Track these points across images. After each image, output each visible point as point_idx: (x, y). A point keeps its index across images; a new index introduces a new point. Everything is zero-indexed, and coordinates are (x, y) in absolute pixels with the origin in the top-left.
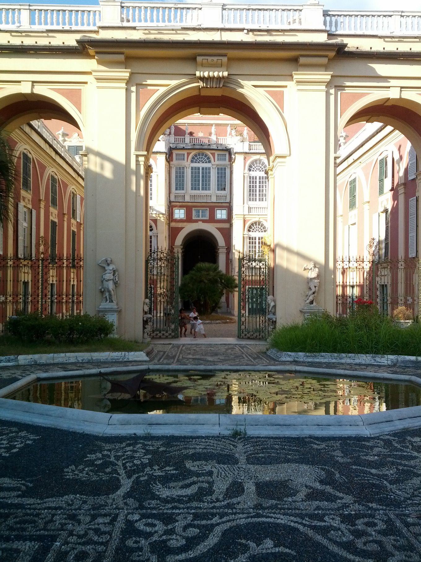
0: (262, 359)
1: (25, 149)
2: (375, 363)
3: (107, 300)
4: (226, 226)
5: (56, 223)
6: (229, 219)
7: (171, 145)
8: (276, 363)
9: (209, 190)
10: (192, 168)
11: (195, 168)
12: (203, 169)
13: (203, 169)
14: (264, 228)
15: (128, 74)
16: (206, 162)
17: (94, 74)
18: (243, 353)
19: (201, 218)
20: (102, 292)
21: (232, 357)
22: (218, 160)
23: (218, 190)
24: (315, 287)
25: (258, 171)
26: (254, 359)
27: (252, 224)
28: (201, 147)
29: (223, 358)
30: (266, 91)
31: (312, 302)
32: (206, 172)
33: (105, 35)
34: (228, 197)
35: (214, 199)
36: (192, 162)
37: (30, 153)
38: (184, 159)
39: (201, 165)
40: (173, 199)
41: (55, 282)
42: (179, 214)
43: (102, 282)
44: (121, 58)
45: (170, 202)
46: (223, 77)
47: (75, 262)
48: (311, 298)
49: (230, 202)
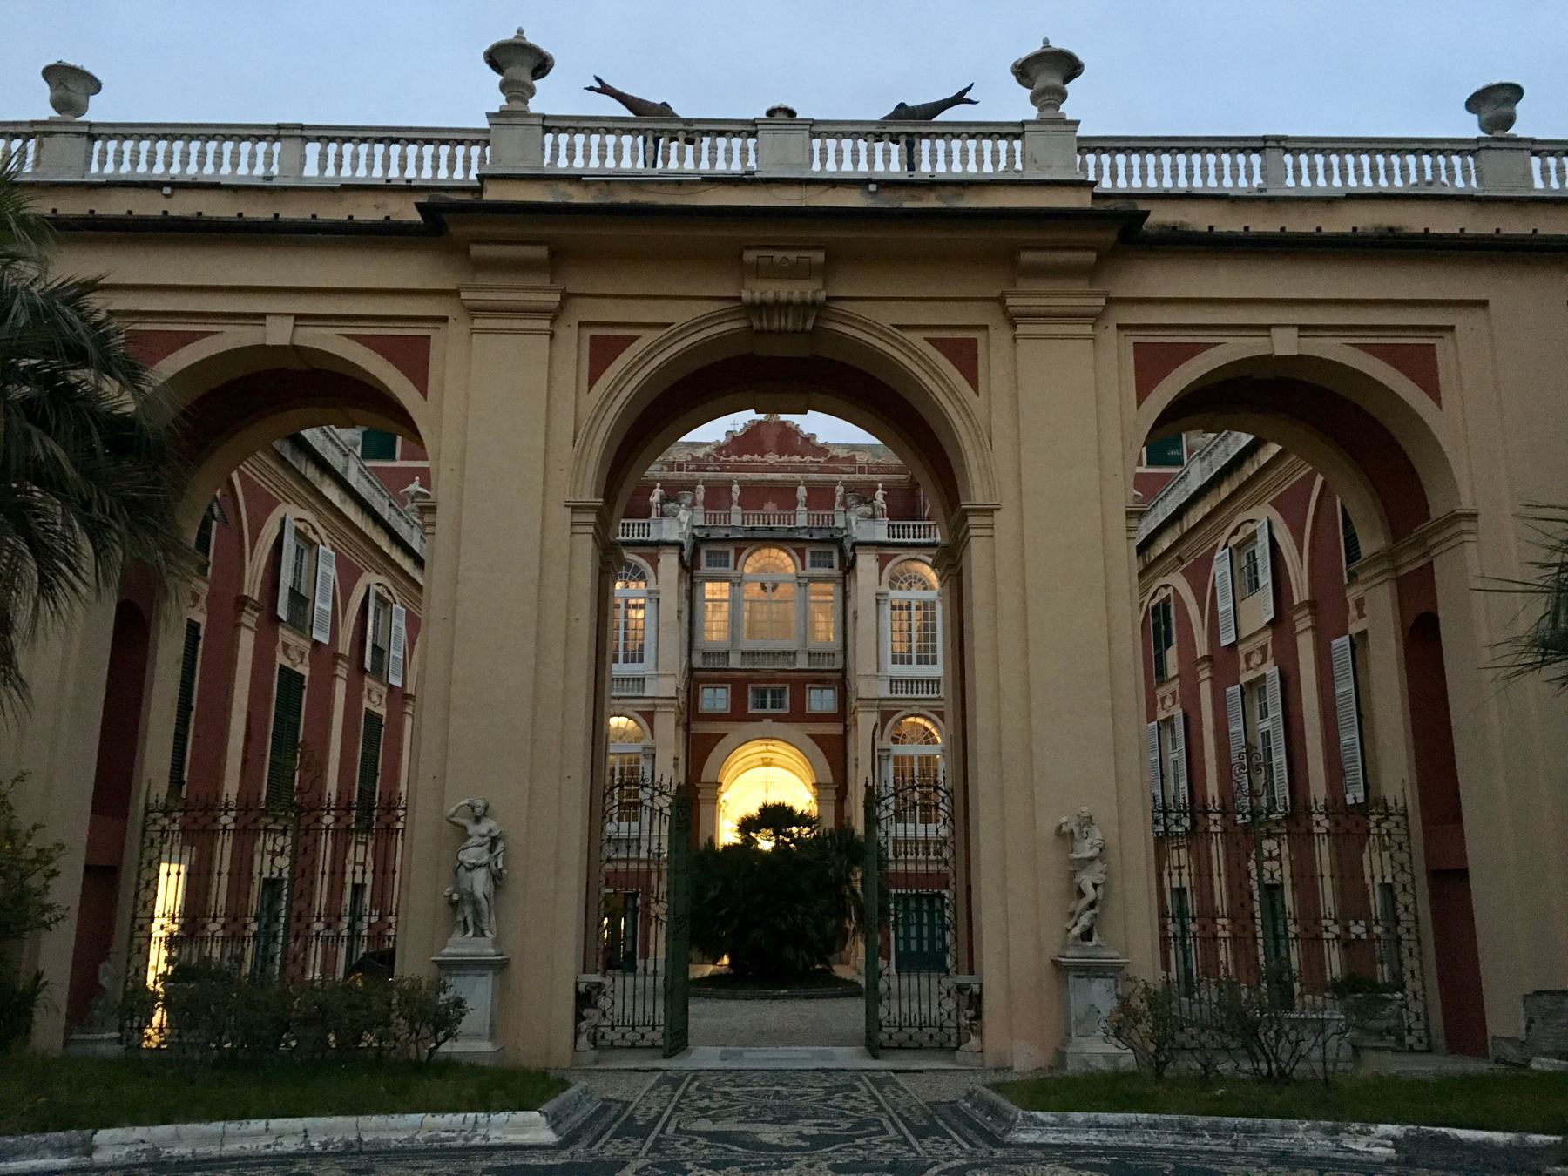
0: (946, 1135)
1: (300, 520)
2: (1339, 1155)
3: (466, 930)
4: (834, 729)
5: (380, 718)
6: (843, 714)
7: (696, 532)
8: (999, 1153)
15: (557, 297)
17: (464, 295)
18: (881, 1109)
19: (769, 710)
20: (454, 905)
21: (845, 1124)
22: (813, 565)
24: (1095, 886)
26: (921, 1134)
29: (814, 1131)
30: (926, 339)
31: (1087, 935)
33: (493, 194)
34: (839, 660)
35: (802, 663)
37: (316, 532)
38: (727, 565)
40: (698, 661)
41: (369, 880)
42: (715, 699)
43: (456, 872)
44: (542, 252)
45: (691, 670)
46: (814, 303)
47: (373, 812)
48: (1084, 921)
49: (844, 671)
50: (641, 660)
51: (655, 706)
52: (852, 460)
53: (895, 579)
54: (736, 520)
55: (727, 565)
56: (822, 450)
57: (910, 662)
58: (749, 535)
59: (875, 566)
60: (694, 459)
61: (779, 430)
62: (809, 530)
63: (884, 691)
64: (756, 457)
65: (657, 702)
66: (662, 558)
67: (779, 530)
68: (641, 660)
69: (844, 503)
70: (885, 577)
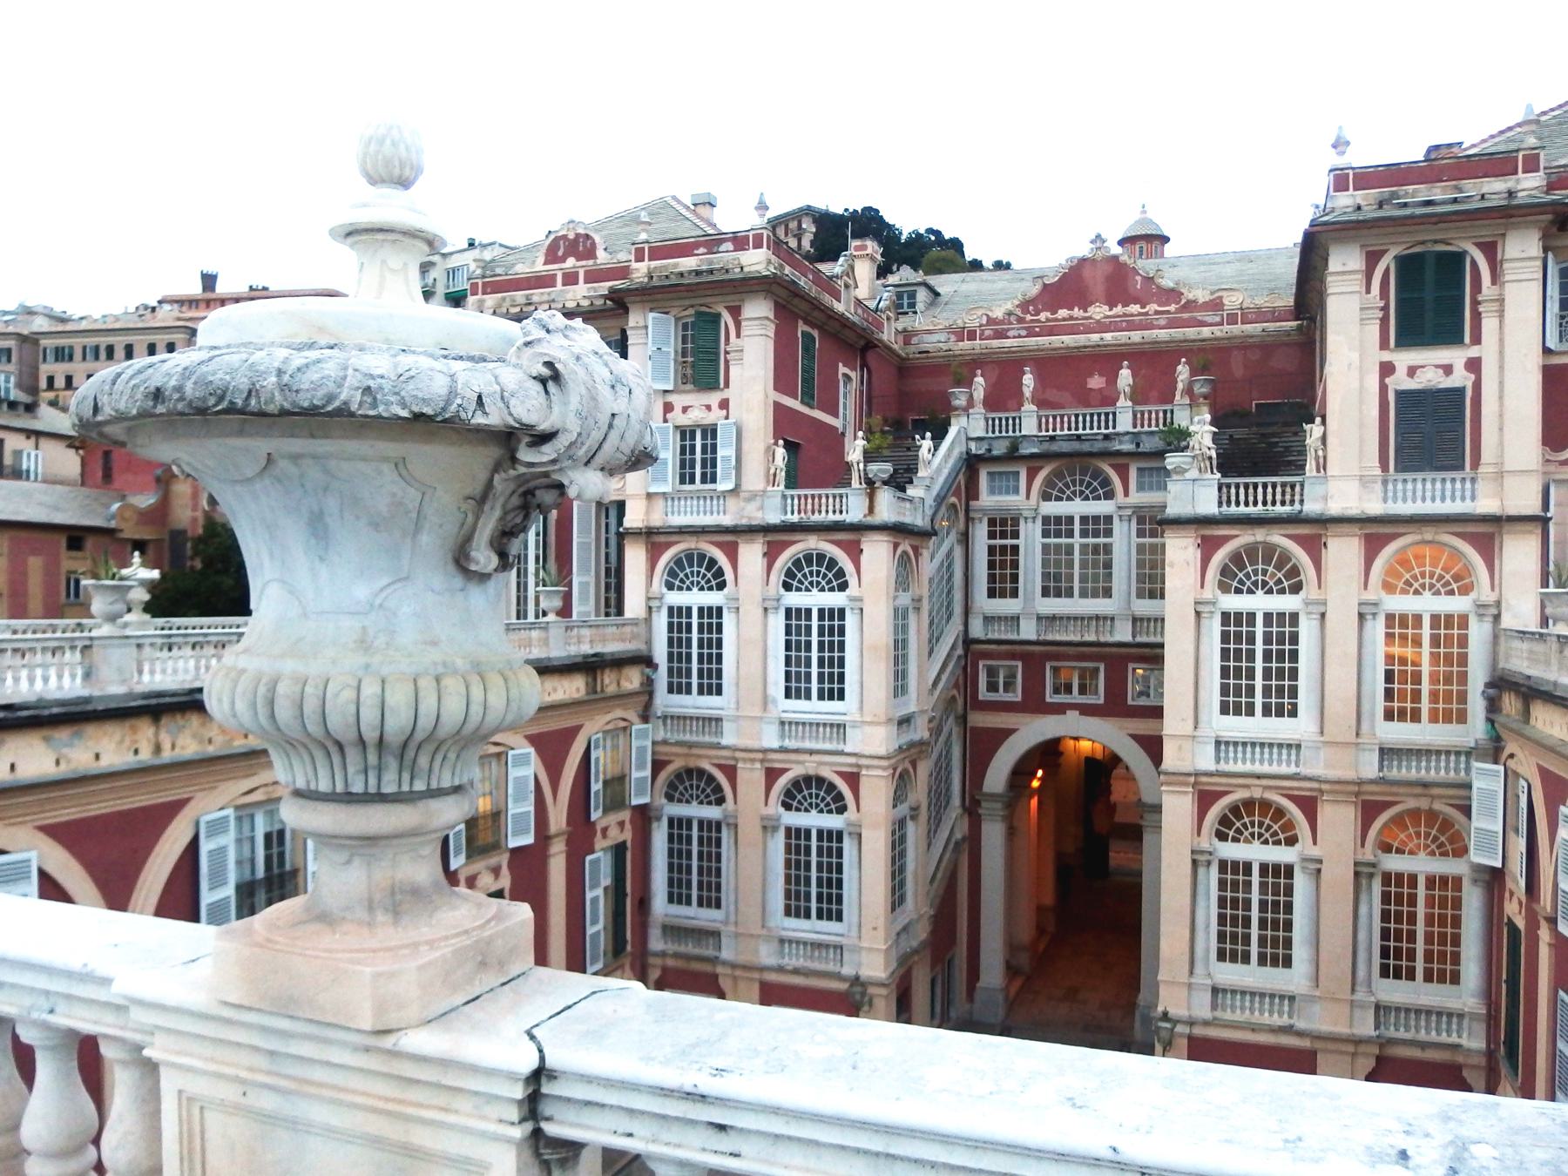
7: (973, 445)
9: (1108, 593)
11: (1058, 520)
13: (1084, 519)
14: (1284, 829)
19: (1076, 697)
22: (1140, 488)
23: (1140, 595)
25: (1260, 592)
28: (1076, 446)
36: (1046, 497)
38: (1016, 491)
39: (1077, 508)
40: (977, 630)
45: (968, 642)
50: (841, 697)
51: (858, 766)
52: (1216, 305)
53: (1225, 571)
54: (1029, 426)
55: (1016, 491)
56: (1172, 294)
58: (1046, 447)
60: (991, 321)
61: (1108, 269)
62: (1136, 437)
63: (1205, 760)
64: (1077, 312)
67: (1091, 439)
68: (841, 697)
69: (1189, 391)
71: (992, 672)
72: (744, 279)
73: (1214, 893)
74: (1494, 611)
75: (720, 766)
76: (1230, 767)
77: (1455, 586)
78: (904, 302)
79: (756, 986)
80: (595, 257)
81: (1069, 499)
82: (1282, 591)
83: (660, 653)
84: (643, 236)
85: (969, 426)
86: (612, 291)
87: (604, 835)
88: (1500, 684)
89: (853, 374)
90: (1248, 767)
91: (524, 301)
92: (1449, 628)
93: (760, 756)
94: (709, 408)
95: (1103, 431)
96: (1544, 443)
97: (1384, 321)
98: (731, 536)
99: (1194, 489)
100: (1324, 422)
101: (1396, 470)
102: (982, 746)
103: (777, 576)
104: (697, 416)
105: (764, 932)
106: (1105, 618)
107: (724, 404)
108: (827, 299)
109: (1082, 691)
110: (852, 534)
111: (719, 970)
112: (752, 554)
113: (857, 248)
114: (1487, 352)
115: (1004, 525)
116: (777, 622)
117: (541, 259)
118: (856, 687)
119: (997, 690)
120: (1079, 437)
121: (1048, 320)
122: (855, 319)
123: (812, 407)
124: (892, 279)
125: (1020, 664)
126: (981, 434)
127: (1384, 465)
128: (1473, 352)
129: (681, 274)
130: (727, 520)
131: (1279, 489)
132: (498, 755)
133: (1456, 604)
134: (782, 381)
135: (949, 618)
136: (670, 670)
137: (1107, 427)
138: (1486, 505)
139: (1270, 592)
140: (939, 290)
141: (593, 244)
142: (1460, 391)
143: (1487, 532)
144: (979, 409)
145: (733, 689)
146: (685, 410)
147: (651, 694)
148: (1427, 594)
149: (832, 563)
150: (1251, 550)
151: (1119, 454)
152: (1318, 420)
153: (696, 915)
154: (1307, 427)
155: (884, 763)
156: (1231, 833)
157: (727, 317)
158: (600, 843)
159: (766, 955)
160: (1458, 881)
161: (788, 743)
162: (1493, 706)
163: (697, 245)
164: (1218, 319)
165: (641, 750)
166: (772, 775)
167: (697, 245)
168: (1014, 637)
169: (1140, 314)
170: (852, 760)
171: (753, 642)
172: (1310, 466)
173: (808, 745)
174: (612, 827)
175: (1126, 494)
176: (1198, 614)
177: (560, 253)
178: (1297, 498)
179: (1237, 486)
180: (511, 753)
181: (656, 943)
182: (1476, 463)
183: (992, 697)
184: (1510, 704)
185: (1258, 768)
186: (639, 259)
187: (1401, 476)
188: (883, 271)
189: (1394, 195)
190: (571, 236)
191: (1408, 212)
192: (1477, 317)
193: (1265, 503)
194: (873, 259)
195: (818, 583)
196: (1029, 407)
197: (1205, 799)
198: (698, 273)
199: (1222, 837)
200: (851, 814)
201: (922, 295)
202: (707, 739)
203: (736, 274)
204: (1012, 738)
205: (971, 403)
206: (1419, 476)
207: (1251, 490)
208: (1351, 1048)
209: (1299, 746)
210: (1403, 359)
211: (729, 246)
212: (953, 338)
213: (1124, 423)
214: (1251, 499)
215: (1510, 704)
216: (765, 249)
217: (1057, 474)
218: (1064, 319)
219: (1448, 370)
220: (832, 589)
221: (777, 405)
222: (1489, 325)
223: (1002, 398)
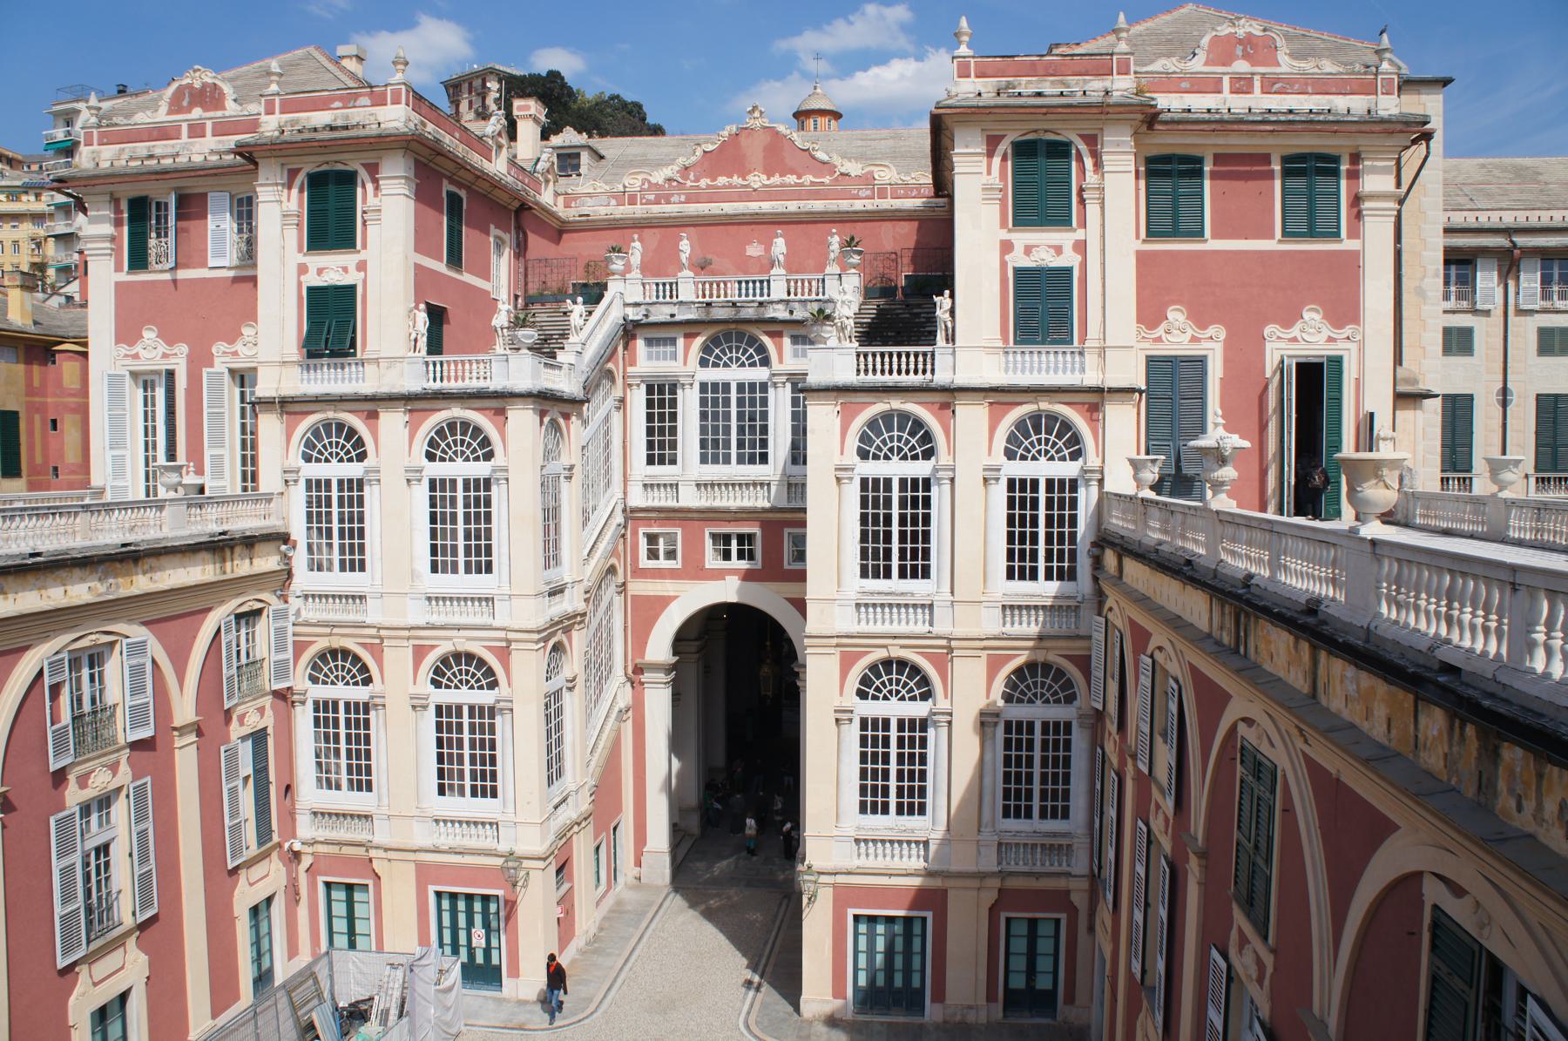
9: (764, 459)
10: (703, 387)
11: (715, 386)
12: (741, 387)
16: (753, 365)
27: (873, 668)
32: (754, 395)
36: (703, 363)
39: (735, 375)
40: (638, 499)
51: (509, 642)
52: (868, 179)
57: (888, 575)
59: (837, 422)
64: (736, 180)
65: (511, 636)
66: (510, 414)
70: (853, 442)
71: (652, 539)
72: (380, 136)
73: (856, 749)
74: (1099, 476)
75: (363, 645)
76: (871, 628)
77: (1066, 452)
78: (568, 161)
79: (413, 866)
80: (224, 108)
81: (726, 365)
82: (915, 457)
83: (298, 529)
84: (274, 88)
85: (627, 293)
86: (240, 145)
87: (241, 723)
88: (1103, 540)
89: (506, 237)
90: (887, 628)
91: (145, 153)
92: (1064, 490)
93: (406, 633)
94: (345, 270)
95: (758, 298)
96: (1139, 320)
97: (1003, 201)
98: (372, 405)
99: (836, 359)
100: (952, 296)
101: (1015, 343)
102: (645, 612)
103: (421, 446)
104: (333, 278)
105: (415, 812)
106: (762, 485)
107: (362, 266)
108: (476, 159)
109: (741, 556)
110: (498, 401)
111: (373, 853)
112: (393, 422)
113: (520, 108)
114: (1092, 234)
115: (661, 396)
116: (422, 493)
117: (164, 108)
118: (505, 559)
119: (657, 558)
120: (734, 304)
121: (709, 187)
122: (510, 179)
123: (459, 271)
124: (556, 140)
125: (679, 531)
126: (639, 299)
127: (1006, 341)
128: (1080, 234)
129: (315, 130)
130: (367, 388)
131: (912, 358)
132: (112, 644)
133: (1067, 469)
134: (422, 243)
135: (608, 485)
136: (310, 546)
137: (762, 295)
138: (1091, 378)
139: (905, 458)
140: (603, 152)
141: (222, 94)
142: (1069, 271)
143: (1095, 398)
144: (636, 274)
145: (378, 565)
146: (320, 271)
147: (290, 574)
148: (1043, 459)
149: (477, 430)
150: (887, 417)
151: (773, 321)
152: (947, 292)
153: (347, 800)
154: (937, 299)
155: (536, 636)
156: (871, 691)
157: (363, 174)
158: (236, 731)
159: (423, 835)
160: (1068, 725)
161: (436, 619)
162: (1097, 563)
163: (332, 99)
164: (869, 193)
165: (281, 632)
166: (420, 653)
167: (332, 99)
168: (671, 503)
169: (797, 185)
170: (502, 634)
171: (397, 517)
172: (940, 337)
173: (457, 619)
174: (254, 715)
175: (781, 361)
176: (838, 480)
177: (185, 103)
178: (929, 367)
179: (874, 355)
180: (125, 641)
181: (306, 829)
182: (1083, 340)
183: (652, 564)
184: (1110, 559)
185: (896, 628)
186: (270, 112)
187: (1019, 348)
188: (545, 136)
189: (1009, 85)
190: (197, 85)
191: (1021, 101)
192: (1082, 201)
193: (899, 372)
194: (536, 120)
195: (463, 453)
196: (687, 273)
197: (847, 662)
198: (332, 128)
199: (862, 695)
200: (503, 690)
201: (585, 157)
202: (352, 617)
203: (373, 130)
204: (673, 606)
205: (628, 268)
206: (1035, 348)
207: (887, 359)
208: (975, 883)
209: (931, 606)
210: (1022, 238)
211: (365, 101)
212: (613, 202)
213: (778, 290)
214: (887, 367)
215: (1110, 559)
216: (403, 106)
217: (715, 341)
218: (724, 187)
219: (1058, 250)
220: (477, 459)
221: (418, 267)
222: (1092, 210)
223: (659, 266)
